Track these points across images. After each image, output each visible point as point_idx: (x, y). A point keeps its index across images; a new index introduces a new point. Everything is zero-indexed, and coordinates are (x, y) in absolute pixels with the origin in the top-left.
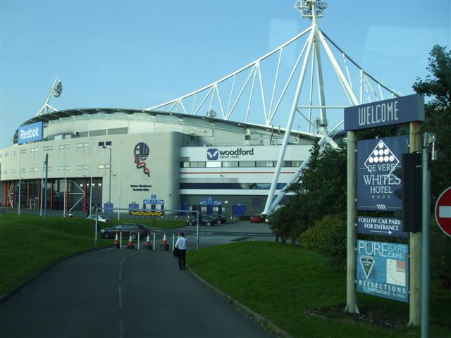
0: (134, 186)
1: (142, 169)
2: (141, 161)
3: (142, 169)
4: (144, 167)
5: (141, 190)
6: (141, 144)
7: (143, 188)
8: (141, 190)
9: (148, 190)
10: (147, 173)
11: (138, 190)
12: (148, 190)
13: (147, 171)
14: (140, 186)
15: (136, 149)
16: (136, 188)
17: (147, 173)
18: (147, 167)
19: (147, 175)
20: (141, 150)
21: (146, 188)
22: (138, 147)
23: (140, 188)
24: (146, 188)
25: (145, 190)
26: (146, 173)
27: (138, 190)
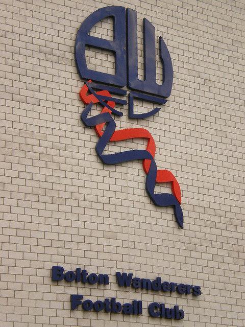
0: (80, 277)
1: (134, 173)
3: (134, 173)
4: (145, 158)
5: (134, 309)
6: (121, 18)
7: (147, 299)
8: (134, 309)
9: (176, 314)
10: (165, 196)
11: (110, 307)
14: (124, 281)
15: (85, 41)
16: (94, 295)
17: (165, 196)
18: (162, 162)
19: (167, 215)
20: (121, 50)
21: (170, 301)
22: (104, 32)
23: (126, 297)
25: (158, 312)
26: (158, 201)
27: (110, 307)
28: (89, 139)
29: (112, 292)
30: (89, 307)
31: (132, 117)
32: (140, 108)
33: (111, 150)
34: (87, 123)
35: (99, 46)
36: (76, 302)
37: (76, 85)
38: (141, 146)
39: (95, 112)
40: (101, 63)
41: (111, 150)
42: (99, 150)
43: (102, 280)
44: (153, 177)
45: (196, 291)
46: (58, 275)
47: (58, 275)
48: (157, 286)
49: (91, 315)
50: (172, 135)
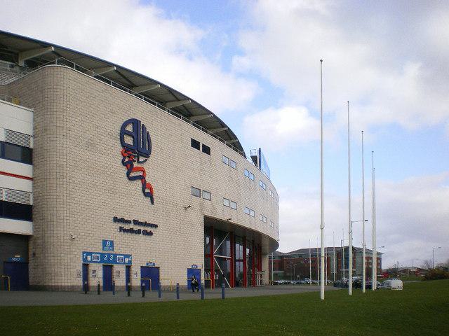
0: (122, 220)
1: (139, 183)
2: (136, 165)
3: (139, 183)
4: (142, 178)
6: (135, 123)
7: (142, 228)
8: (138, 232)
10: (148, 193)
11: (131, 231)
12: (150, 234)
13: (147, 191)
14: (136, 222)
15: (123, 132)
16: (127, 227)
17: (148, 193)
18: (148, 180)
21: (149, 229)
22: (129, 128)
23: (136, 228)
24: (149, 229)
25: (146, 233)
26: (146, 195)
27: (131, 231)
28: (124, 170)
29: (132, 226)
30: (125, 231)
31: (138, 162)
32: (142, 159)
33: (132, 175)
34: (124, 163)
35: (129, 134)
36: (121, 229)
37: (120, 148)
38: (141, 174)
39: (127, 160)
40: (129, 141)
41: (132, 175)
42: (128, 175)
43: (129, 222)
44: (145, 185)
45: (156, 226)
46: (116, 220)
47: (116, 220)
48: (145, 224)
49: (126, 233)
50: (152, 168)
